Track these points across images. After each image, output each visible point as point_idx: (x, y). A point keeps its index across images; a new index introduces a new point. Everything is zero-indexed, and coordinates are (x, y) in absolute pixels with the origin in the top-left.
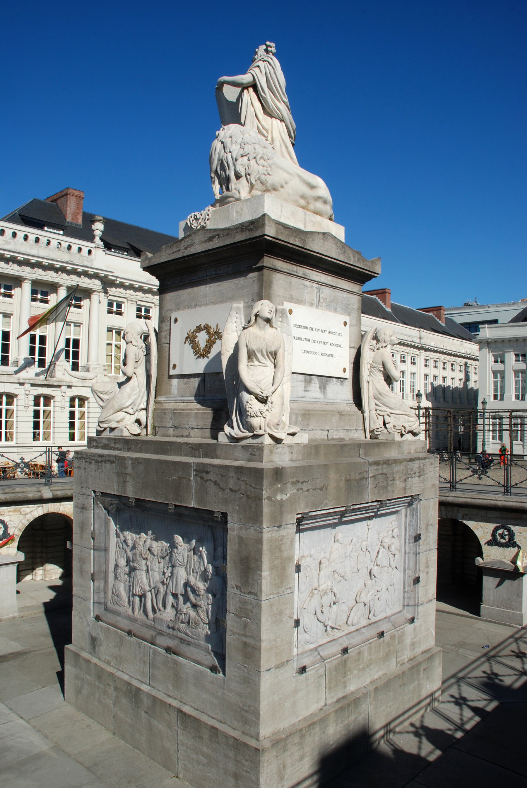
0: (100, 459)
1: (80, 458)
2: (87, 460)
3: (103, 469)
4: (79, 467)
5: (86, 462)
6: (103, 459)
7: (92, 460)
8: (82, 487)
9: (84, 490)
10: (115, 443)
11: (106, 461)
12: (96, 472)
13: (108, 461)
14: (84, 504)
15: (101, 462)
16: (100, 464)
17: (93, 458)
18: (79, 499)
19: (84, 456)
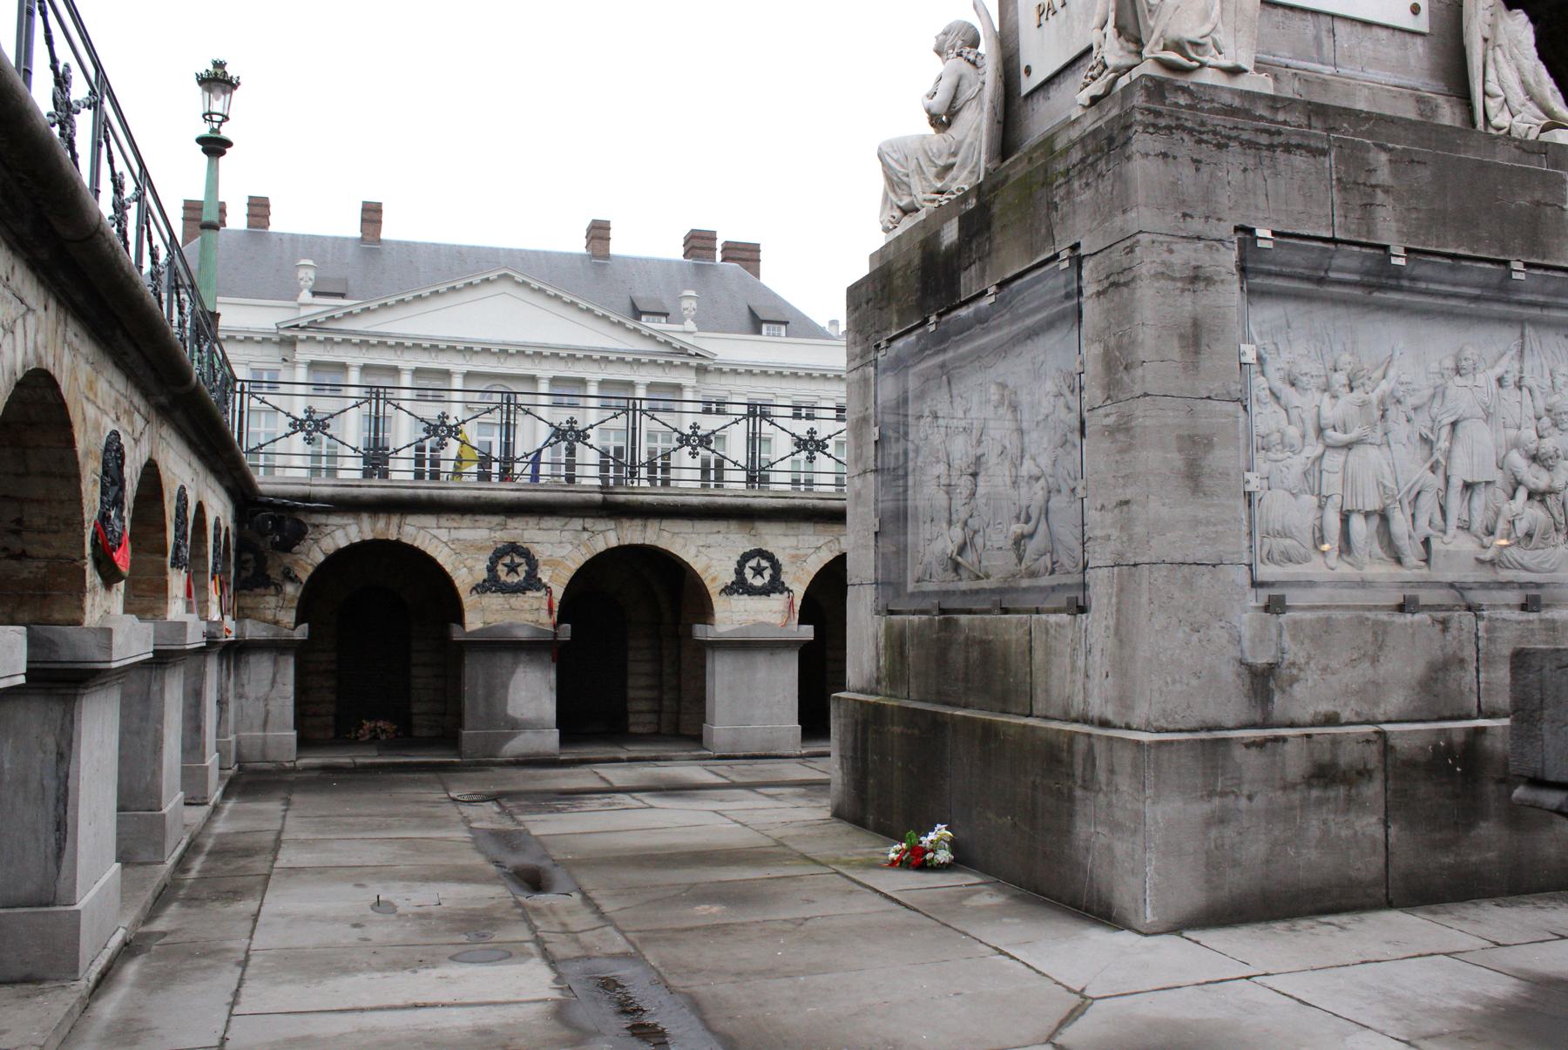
0: (1264, 139)
1: (1169, 128)
2: (1205, 137)
3: (1281, 167)
4: (1165, 155)
5: (1200, 142)
6: (1281, 139)
7: (1229, 138)
8: (1185, 215)
9: (1196, 226)
10: (1275, 109)
11: (1288, 148)
12: (1250, 175)
13: (1298, 146)
14: (1196, 268)
15: (1271, 147)
16: (1265, 153)
17: (1234, 133)
18: (1171, 251)
19: (1189, 124)
